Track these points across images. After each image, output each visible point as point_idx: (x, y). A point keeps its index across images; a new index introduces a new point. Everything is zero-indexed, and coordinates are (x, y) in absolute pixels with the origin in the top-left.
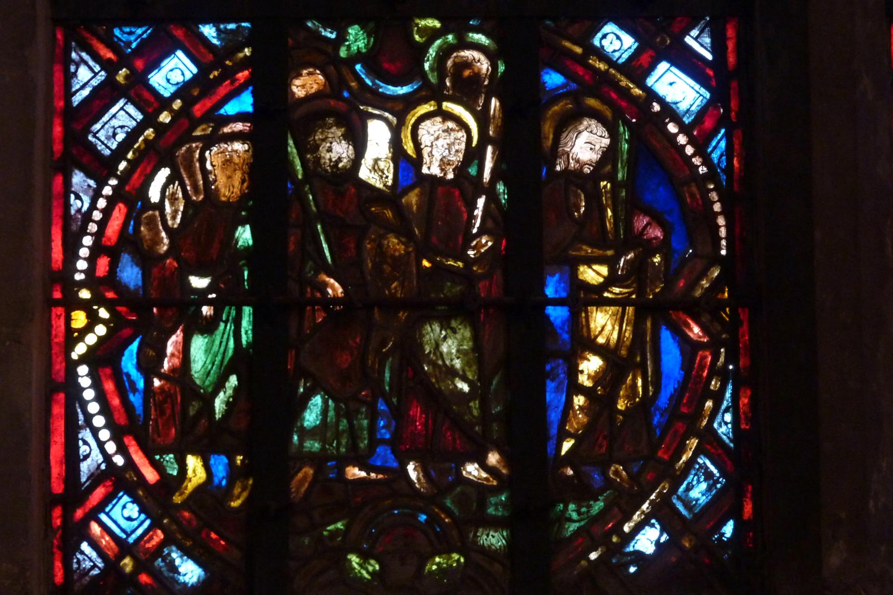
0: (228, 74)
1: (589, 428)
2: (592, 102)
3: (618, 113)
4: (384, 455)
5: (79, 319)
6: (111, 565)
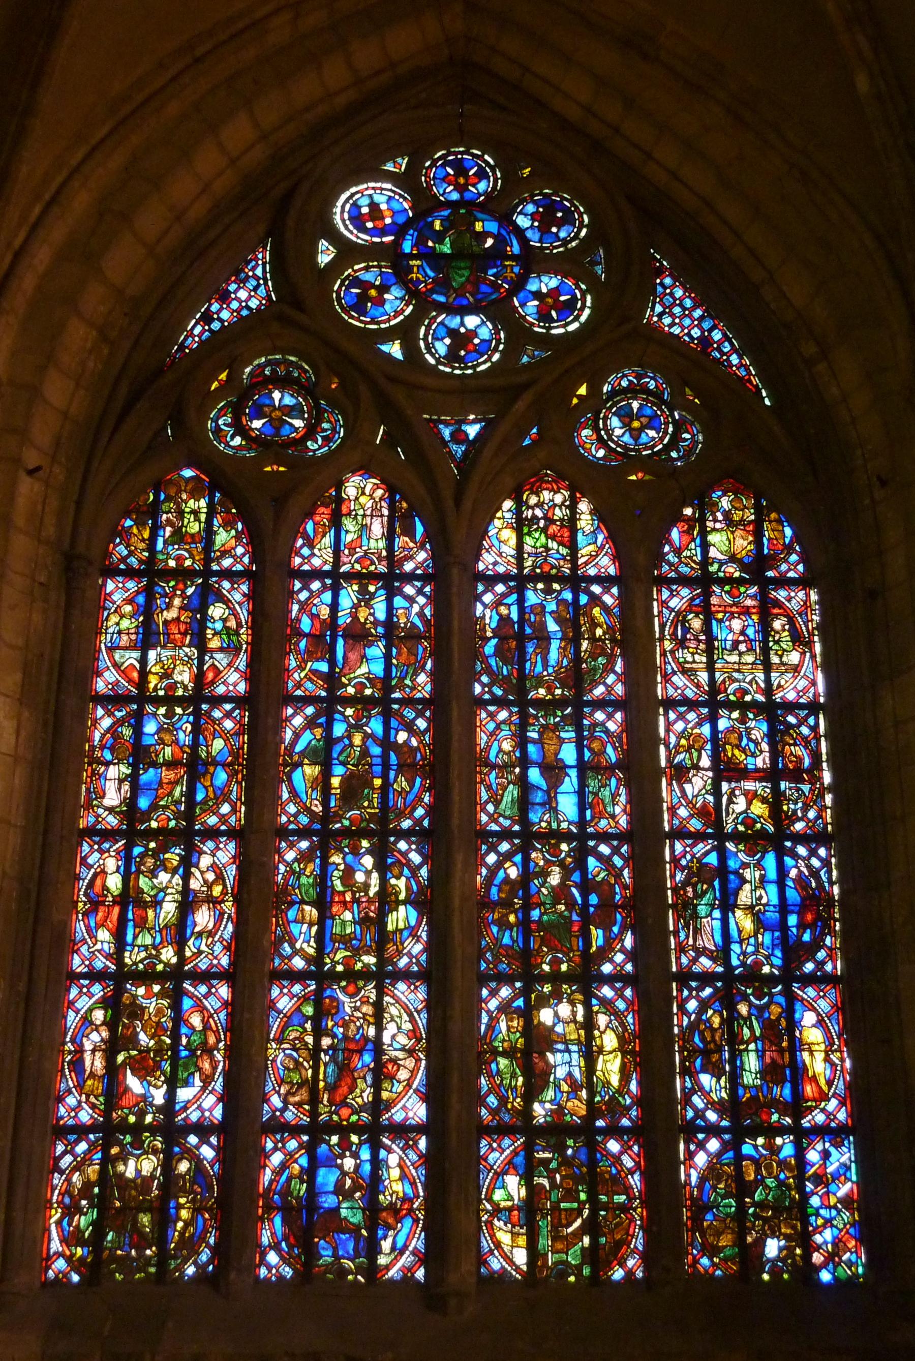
0: (96, 1148)
1: (179, 1241)
2: (186, 1155)
3: (192, 1158)
4: (127, 1248)
5: (53, 1212)
6: (57, 1276)
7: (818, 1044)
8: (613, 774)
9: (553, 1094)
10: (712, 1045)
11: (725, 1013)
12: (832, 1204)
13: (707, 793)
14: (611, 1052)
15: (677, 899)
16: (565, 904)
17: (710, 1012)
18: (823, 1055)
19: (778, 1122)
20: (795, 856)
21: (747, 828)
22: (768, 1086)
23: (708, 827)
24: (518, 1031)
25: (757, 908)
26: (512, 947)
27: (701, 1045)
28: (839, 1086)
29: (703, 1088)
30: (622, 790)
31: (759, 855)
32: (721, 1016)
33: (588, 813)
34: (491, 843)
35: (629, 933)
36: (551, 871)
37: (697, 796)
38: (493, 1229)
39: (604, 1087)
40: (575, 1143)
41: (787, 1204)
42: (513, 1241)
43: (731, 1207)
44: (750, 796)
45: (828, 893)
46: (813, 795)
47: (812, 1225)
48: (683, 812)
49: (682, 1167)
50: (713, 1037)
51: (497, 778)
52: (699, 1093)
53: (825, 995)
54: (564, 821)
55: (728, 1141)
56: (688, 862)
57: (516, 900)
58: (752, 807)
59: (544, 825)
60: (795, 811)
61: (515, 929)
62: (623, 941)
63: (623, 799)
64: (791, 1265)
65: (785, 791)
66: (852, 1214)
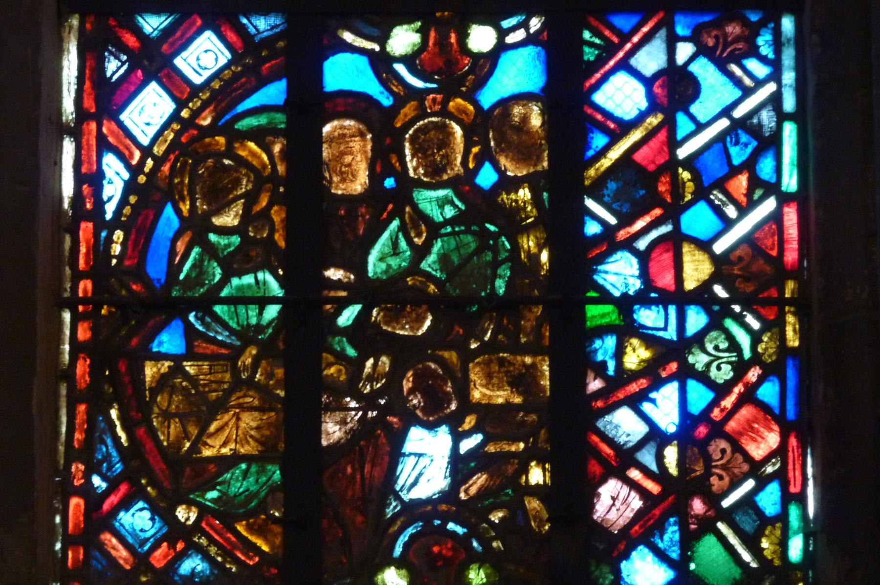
12: (690, 284)
41: (500, 286)
43: (263, 302)
47: (600, 369)
49: (68, 147)
55: (269, 42)
64: (501, 529)
66: (775, 325)
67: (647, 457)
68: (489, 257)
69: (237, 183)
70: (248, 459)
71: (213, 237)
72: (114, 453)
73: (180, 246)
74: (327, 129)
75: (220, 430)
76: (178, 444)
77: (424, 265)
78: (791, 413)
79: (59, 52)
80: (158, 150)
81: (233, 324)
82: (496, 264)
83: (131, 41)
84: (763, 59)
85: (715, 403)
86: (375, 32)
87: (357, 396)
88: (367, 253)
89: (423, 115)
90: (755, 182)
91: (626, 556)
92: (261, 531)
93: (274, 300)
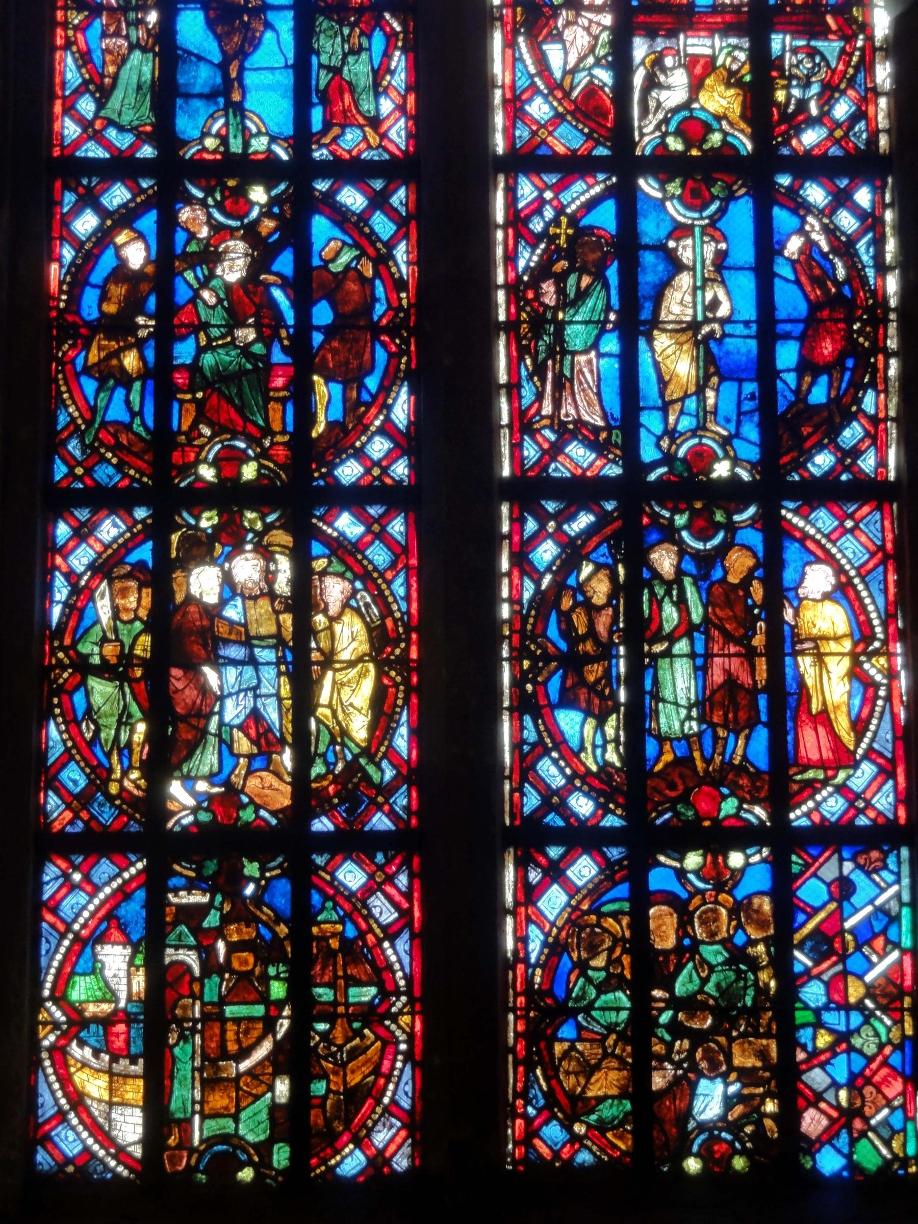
7: (837, 639)
8: (380, 23)
9: (215, 759)
10: (589, 647)
11: (621, 570)
12: (852, 1000)
13: (598, 63)
14: (351, 664)
15: (520, 309)
16: (257, 326)
17: (587, 569)
18: (846, 663)
19: (737, 816)
20: (800, 208)
21: (689, 145)
22: (716, 738)
23: (598, 143)
24: (137, 618)
25: (706, 329)
26: (128, 427)
27: (563, 646)
28: (881, 733)
29: (565, 742)
30: (398, 60)
31: (714, 207)
32: (613, 577)
33: (317, 116)
34: (88, 188)
35: (405, 389)
36: (226, 251)
37: (574, 71)
38: (66, 1066)
39: (333, 742)
40: (263, 870)
41: (749, 1001)
42: (111, 1091)
43: (618, 1009)
44: (698, 70)
45: (874, 293)
46: (848, 64)
47: (804, 1047)
48: (539, 109)
49: (509, 921)
50: (591, 625)
51: (104, 35)
52: (555, 755)
53: (856, 527)
54: (259, 133)
55: (618, 862)
56: (547, 225)
57: (141, 320)
58: (703, 97)
59: (210, 143)
60: (802, 105)
61: (137, 385)
62: (389, 408)
63: (399, 79)
64: (751, 1137)
65: (781, 58)
66: (899, 1022)
67: (830, 1096)
68: (742, 984)
69: (603, 941)
70: (613, 1097)
71: (590, 973)
72: (539, 1094)
73: (573, 978)
74: (652, 911)
75: (597, 1081)
76: (575, 1088)
77: (706, 989)
78: (908, 1070)
79: (502, 867)
80: (560, 923)
81: (602, 1021)
82: (746, 988)
83: (543, 860)
84: (892, 872)
85: (867, 1066)
86: (676, 855)
87: (672, 1062)
88: (674, 982)
89: (704, 903)
90: (888, 941)
91: (819, 1151)
92: (621, 1138)
93: (624, 1009)
